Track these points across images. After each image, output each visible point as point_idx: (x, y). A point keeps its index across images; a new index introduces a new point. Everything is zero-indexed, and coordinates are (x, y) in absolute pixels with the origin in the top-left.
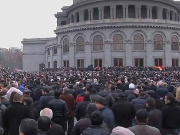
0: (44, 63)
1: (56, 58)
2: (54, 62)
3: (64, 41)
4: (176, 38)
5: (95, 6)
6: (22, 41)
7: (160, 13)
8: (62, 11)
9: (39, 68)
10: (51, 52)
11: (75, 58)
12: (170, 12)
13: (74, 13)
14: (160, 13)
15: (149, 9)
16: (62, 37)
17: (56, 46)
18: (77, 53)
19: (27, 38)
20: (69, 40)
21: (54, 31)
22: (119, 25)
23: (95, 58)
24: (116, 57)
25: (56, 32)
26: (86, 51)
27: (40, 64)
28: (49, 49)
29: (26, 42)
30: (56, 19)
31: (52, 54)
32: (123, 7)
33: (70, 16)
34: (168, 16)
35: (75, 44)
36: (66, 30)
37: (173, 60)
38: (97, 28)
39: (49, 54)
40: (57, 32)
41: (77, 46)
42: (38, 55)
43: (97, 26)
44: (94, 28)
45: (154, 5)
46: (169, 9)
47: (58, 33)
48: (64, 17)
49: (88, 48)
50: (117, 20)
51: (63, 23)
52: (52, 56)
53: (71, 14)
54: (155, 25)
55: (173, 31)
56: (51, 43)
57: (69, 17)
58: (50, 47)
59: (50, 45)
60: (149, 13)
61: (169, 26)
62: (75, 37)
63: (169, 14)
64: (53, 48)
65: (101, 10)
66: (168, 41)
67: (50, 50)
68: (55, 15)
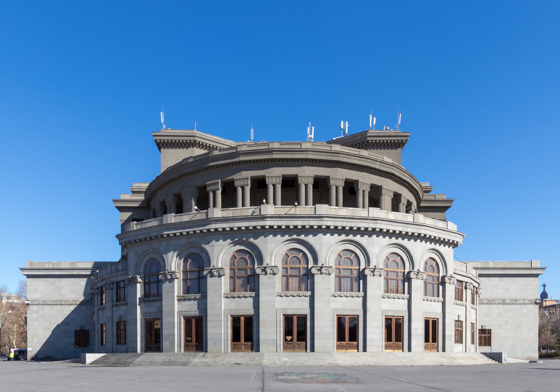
12: (406, 204)
21: (117, 236)
23: (233, 314)
24: (289, 312)
25: (124, 240)
40: (126, 239)
63: (405, 206)
66: (419, 272)
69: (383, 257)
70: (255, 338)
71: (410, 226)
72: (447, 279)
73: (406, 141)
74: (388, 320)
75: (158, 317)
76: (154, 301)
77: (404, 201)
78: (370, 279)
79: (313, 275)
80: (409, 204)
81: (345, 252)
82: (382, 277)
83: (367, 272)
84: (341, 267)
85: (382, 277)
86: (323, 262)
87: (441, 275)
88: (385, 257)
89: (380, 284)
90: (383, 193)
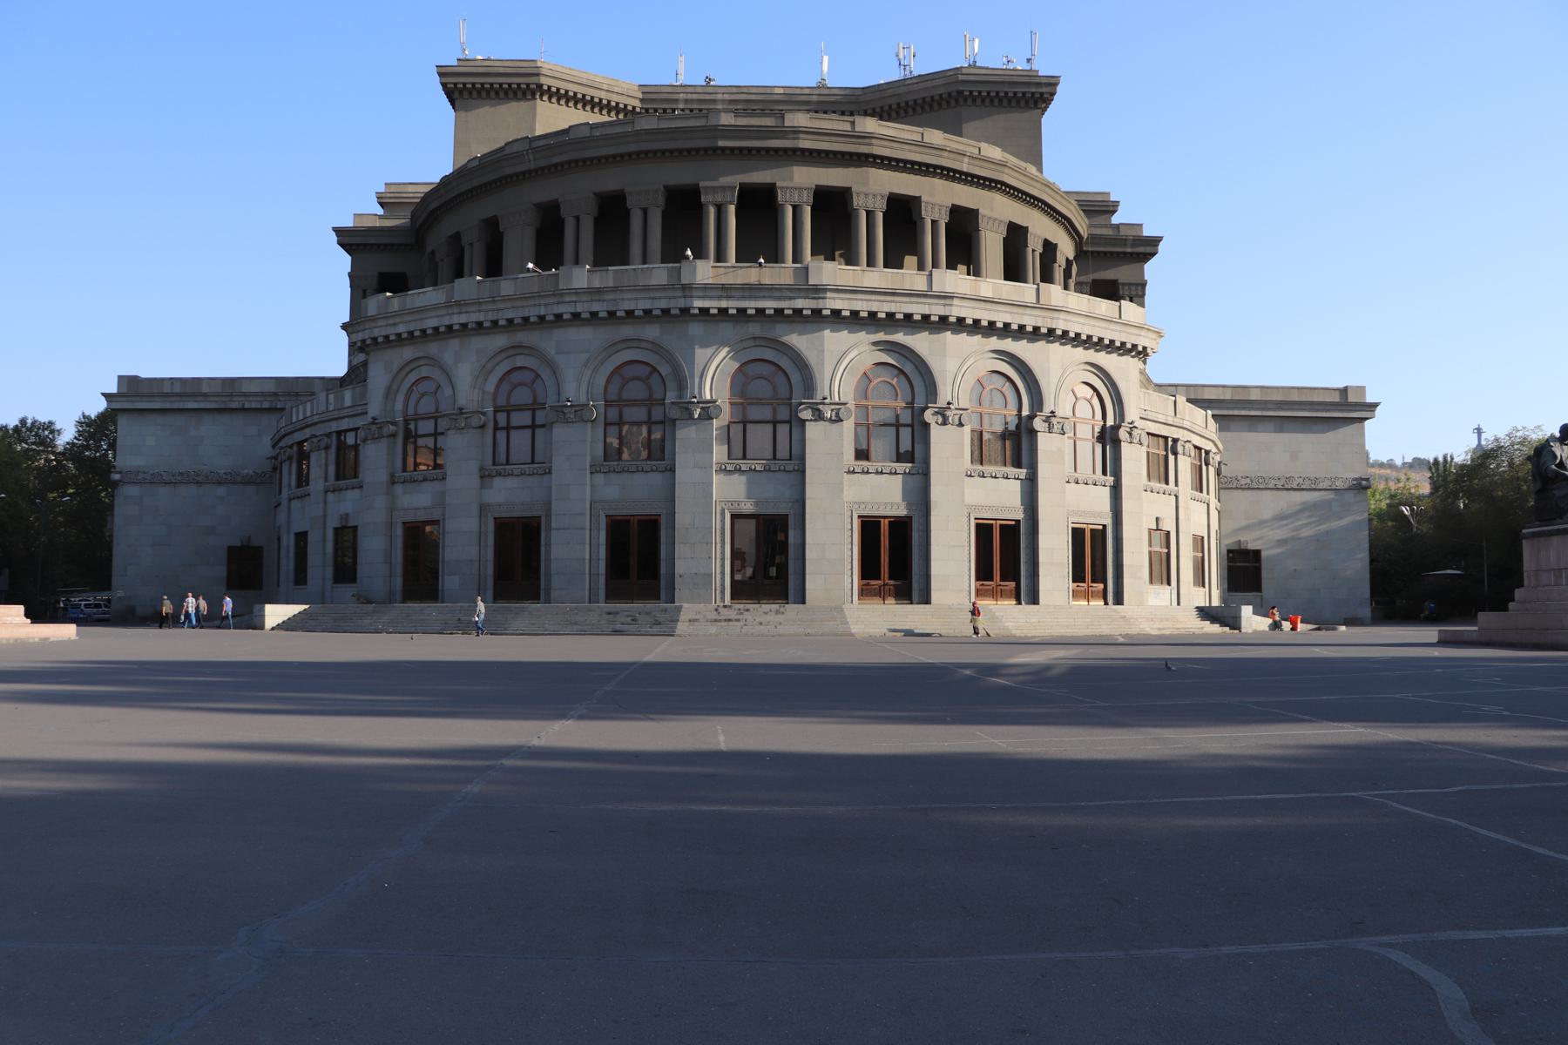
0: (256, 542)
1: (347, 503)
2: (336, 529)
3: (410, 391)
4: (1096, 402)
5: (610, 181)
6: (113, 389)
7: (992, 246)
8: (380, 211)
9: (221, 571)
10: (320, 466)
11: (483, 509)
12: (1040, 249)
13: (467, 221)
14: (992, 246)
15: (934, 222)
16: (395, 367)
17: (356, 429)
18: (499, 474)
19: (144, 375)
20: (448, 392)
22: (770, 305)
23: (612, 513)
26: (560, 464)
27: (231, 550)
28: (300, 444)
29: (137, 399)
30: (345, 261)
31: (326, 479)
32: (780, 199)
33: (437, 240)
34: (1033, 263)
35: (484, 414)
36: (431, 323)
37: (1078, 534)
38: (630, 313)
39: (303, 479)
41: (496, 428)
42: (222, 491)
43: (628, 306)
44: (612, 314)
45: (966, 196)
46: (1041, 228)
47: (375, 339)
48: (395, 255)
49: (576, 447)
50: (751, 274)
51: (395, 283)
52: (326, 491)
53: (448, 226)
54: (985, 316)
55: (1081, 354)
56: (322, 408)
57: (429, 249)
58: (307, 433)
59: (310, 421)
60: (934, 240)
61: (1060, 325)
62: (485, 372)
64: (334, 437)
65: (645, 211)
67: (314, 457)
68: (340, 232)
69: (969, 381)
70: (663, 570)
71: (1028, 311)
72: (1123, 434)
73: (1053, 94)
74: (983, 531)
75: (436, 517)
76: (425, 480)
77: (1035, 245)
78: (936, 433)
79: (803, 422)
80: (1049, 248)
81: (879, 368)
82: (967, 429)
83: (929, 416)
84: (871, 403)
85: (967, 429)
86: (827, 394)
87: (1110, 422)
88: (973, 381)
89: (963, 445)
90: (982, 226)
